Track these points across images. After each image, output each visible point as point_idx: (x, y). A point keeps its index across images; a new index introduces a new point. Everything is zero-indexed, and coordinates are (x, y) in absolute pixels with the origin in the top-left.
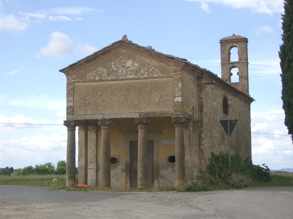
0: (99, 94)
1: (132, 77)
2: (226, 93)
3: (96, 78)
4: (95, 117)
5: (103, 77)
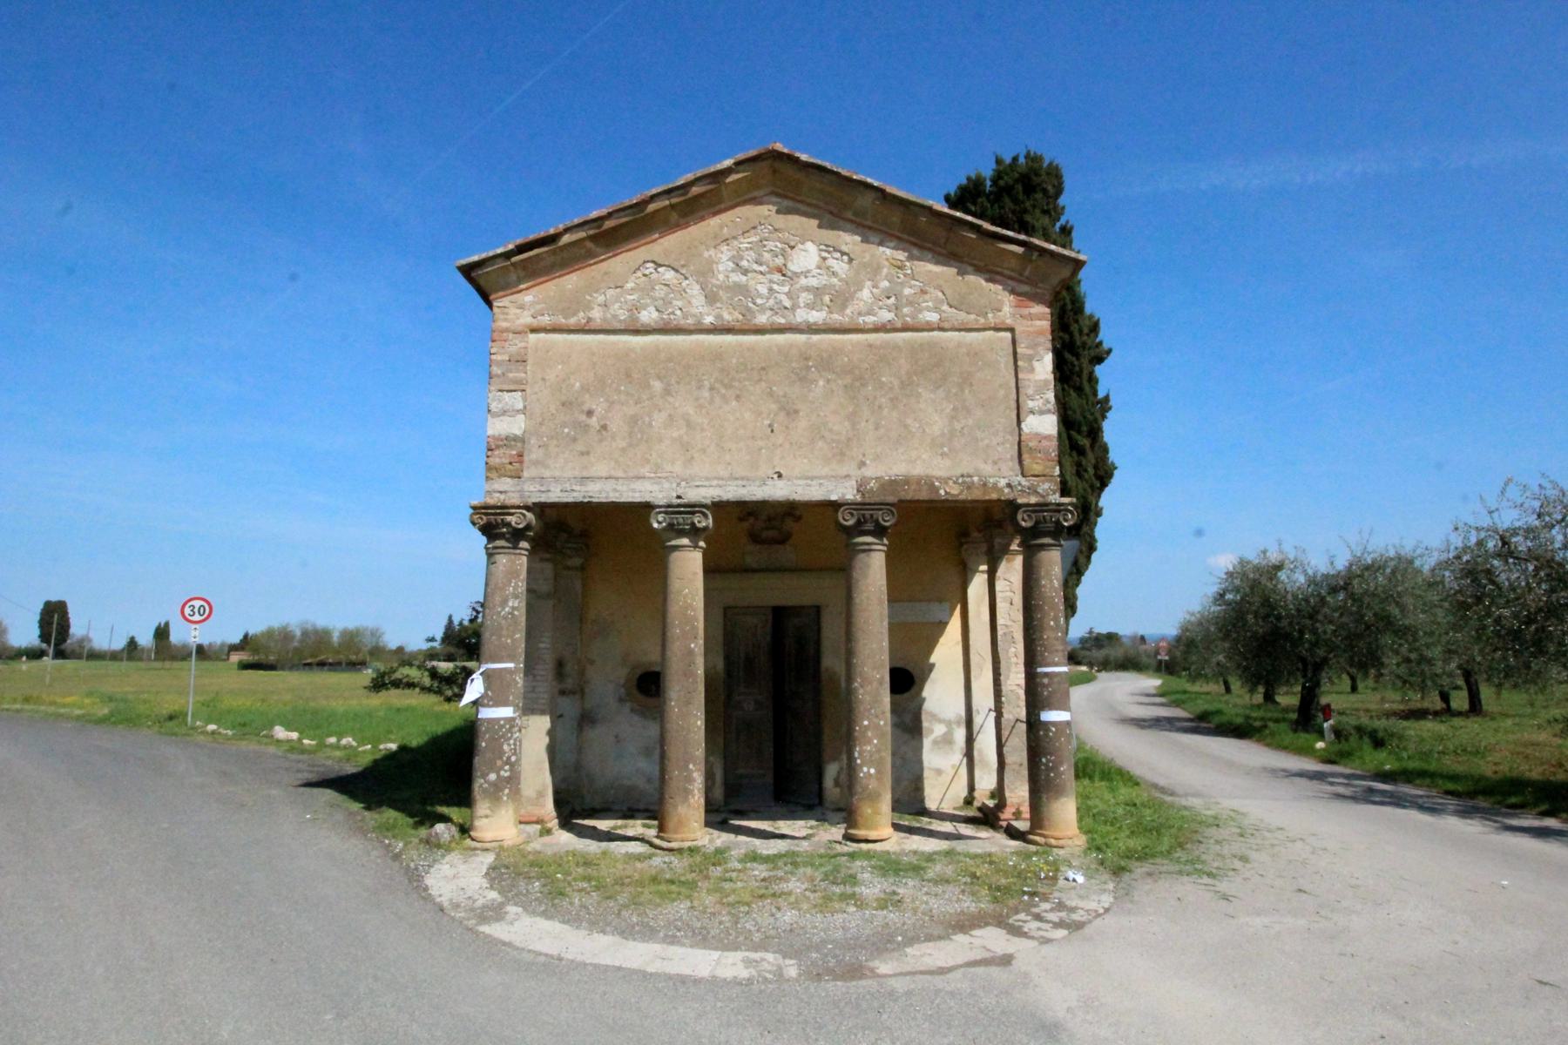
0: (657, 385)
1: (816, 317)
4: (634, 491)
5: (678, 312)
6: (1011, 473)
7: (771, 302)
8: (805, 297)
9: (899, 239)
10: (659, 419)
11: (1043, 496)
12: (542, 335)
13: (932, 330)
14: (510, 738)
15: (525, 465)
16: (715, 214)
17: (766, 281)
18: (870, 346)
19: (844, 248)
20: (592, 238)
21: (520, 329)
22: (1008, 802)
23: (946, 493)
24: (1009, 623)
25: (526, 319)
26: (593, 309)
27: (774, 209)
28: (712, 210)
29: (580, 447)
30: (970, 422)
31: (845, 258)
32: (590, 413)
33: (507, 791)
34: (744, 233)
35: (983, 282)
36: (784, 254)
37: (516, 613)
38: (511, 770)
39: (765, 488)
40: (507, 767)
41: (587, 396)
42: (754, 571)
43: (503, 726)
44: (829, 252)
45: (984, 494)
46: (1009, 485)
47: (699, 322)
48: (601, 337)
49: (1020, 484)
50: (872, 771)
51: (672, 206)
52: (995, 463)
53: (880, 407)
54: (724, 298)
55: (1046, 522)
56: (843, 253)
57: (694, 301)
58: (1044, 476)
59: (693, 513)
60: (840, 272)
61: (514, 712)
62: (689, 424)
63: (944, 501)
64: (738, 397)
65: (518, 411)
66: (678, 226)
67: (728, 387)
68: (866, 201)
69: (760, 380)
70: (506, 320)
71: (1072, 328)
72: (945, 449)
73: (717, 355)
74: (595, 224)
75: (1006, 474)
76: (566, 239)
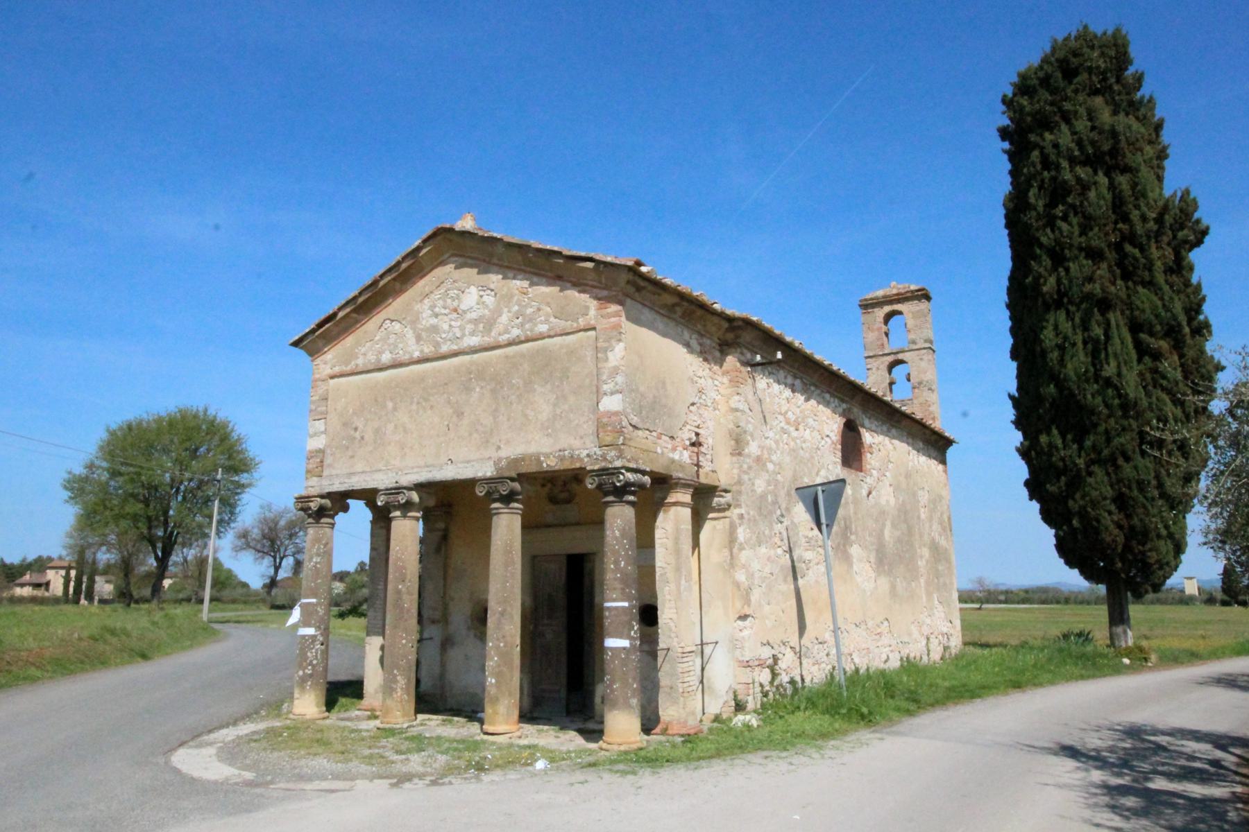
0: (390, 405)
1: (474, 341)
2: (855, 410)
3: (384, 355)
4: (374, 480)
5: (401, 352)
6: (593, 445)
7: (451, 334)
8: (469, 327)
9: (525, 272)
10: (390, 427)
11: (610, 462)
12: (336, 380)
13: (544, 338)
14: (312, 649)
15: (324, 467)
16: (421, 278)
17: (447, 320)
18: (507, 357)
19: (492, 286)
20: (354, 311)
21: (324, 378)
22: (662, 720)
23: (548, 465)
24: (664, 565)
25: (328, 371)
26: (358, 358)
27: (453, 266)
28: (420, 275)
29: (350, 453)
30: (566, 407)
31: (493, 293)
32: (356, 429)
33: (309, 683)
34: (437, 288)
35: (577, 294)
36: (458, 297)
37: (318, 566)
38: (313, 669)
39: (442, 471)
40: (310, 667)
41: (355, 418)
42: (548, 526)
43: (307, 640)
44: (484, 291)
45: (571, 463)
46: (588, 455)
47: (412, 358)
48: (363, 376)
49: (595, 454)
50: (493, 681)
51: (394, 279)
52: (581, 438)
53: (511, 403)
54: (425, 337)
55: (606, 484)
56: (492, 290)
57: (410, 342)
58: (612, 445)
59: (398, 493)
60: (490, 304)
61: (316, 631)
62: (405, 431)
63: (547, 472)
64: (432, 407)
65: (322, 433)
66: (402, 291)
67: (426, 400)
68: (500, 249)
69: (444, 393)
70: (319, 373)
71: (1131, 216)
72: (550, 431)
73: (422, 378)
74: (353, 302)
75: (588, 447)
76: (341, 314)
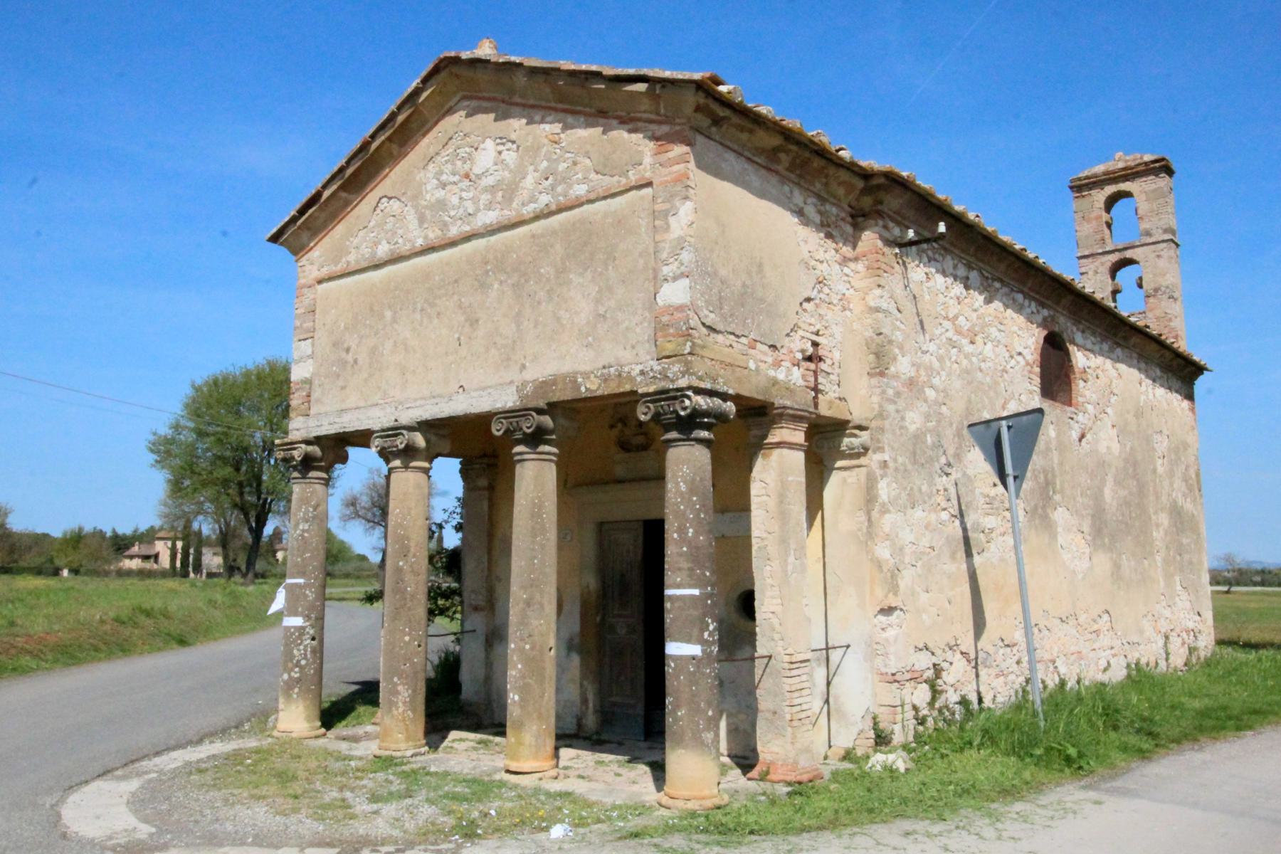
1: (490, 217)
2: (1062, 320)
3: (380, 247)
4: (369, 418)
5: (400, 241)
6: (648, 357)
7: (461, 211)
8: (485, 197)
9: (555, 110)
12: (325, 285)
13: (581, 204)
14: (300, 644)
16: (424, 135)
17: (457, 191)
18: (533, 236)
19: (513, 137)
20: (341, 188)
21: (310, 282)
22: (761, 756)
24: (765, 535)
27: (463, 113)
28: (421, 133)
29: (340, 383)
30: (612, 303)
32: (348, 350)
33: (296, 690)
35: (625, 135)
36: (470, 158)
37: (306, 535)
38: (300, 672)
39: (451, 403)
40: (297, 669)
43: (293, 634)
44: (503, 144)
45: (619, 386)
46: (642, 373)
49: (652, 370)
50: (517, 698)
51: (389, 139)
53: (539, 303)
55: (666, 414)
56: (513, 142)
57: (411, 227)
58: (675, 356)
59: (396, 435)
67: (432, 305)
68: (521, 80)
70: (304, 277)
72: (590, 339)
73: (427, 275)
74: (341, 176)
76: (326, 194)
